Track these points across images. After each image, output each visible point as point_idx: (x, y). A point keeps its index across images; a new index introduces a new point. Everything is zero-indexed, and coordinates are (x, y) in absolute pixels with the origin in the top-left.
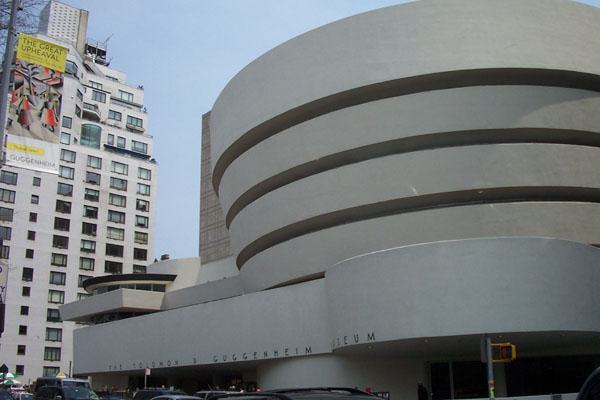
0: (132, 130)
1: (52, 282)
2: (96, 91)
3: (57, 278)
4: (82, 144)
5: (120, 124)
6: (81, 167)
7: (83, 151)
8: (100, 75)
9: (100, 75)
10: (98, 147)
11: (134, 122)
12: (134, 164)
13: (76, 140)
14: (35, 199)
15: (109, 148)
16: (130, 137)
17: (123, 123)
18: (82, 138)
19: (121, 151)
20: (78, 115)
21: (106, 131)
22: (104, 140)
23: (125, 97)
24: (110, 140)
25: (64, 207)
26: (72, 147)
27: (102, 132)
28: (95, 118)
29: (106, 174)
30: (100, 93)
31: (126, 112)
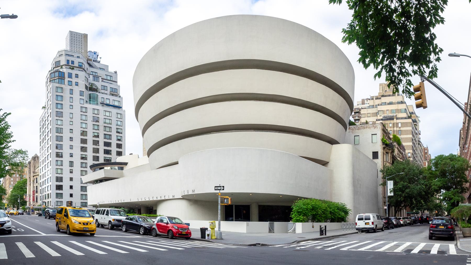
0: (113, 95)
1: (82, 167)
2: (94, 77)
3: (84, 165)
4: (90, 103)
5: (106, 92)
6: (90, 114)
7: (90, 107)
8: (96, 68)
9: (96, 68)
10: (97, 104)
11: (114, 91)
12: (114, 111)
13: (87, 102)
15: (103, 104)
16: (112, 98)
17: (108, 92)
18: (90, 101)
19: (108, 105)
20: (87, 89)
21: (100, 96)
22: (100, 100)
23: (109, 78)
24: (103, 100)
25: (84, 133)
26: (86, 105)
27: (99, 96)
28: (96, 90)
29: (101, 117)
30: (96, 77)
31: (109, 86)
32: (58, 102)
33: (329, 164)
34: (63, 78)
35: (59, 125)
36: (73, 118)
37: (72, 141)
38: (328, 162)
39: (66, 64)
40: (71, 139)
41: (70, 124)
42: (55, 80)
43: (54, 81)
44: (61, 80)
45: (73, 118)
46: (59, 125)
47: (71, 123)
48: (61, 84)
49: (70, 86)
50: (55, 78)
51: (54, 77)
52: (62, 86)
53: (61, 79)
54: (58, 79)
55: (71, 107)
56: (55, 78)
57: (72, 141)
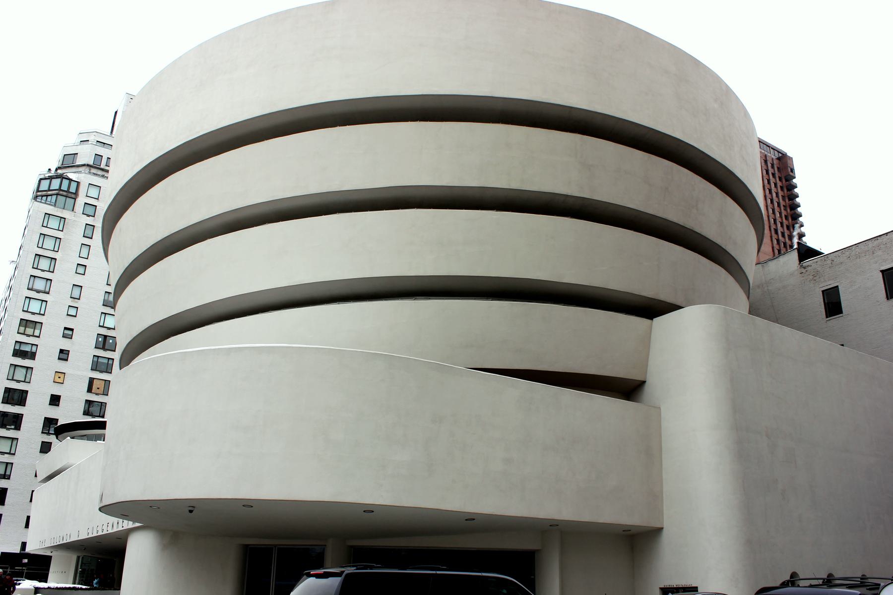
14: (68, 333)
32: (41, 252)
33: (647, 387)
34: (73, 196)
35: (33, 313)
36: (79, 299)
37: (67, 360)
38: (644, 382)
39: (91, 163)
40: (63, 356)
41: (68, 315)
42: (47, 196)
43: (44, 198)
44: (64, 198)
45: (79, 299)
46: (33, 313)
47: (72, 312)
48: (64, 209)
49: (88, 216)
50: (50, 193)
51: (47, 189)
52: (66, 214)
53: (66, 197)
54: (57, 194)
55: (81, 270)
56: (50, 193)
57: (67, 360)
